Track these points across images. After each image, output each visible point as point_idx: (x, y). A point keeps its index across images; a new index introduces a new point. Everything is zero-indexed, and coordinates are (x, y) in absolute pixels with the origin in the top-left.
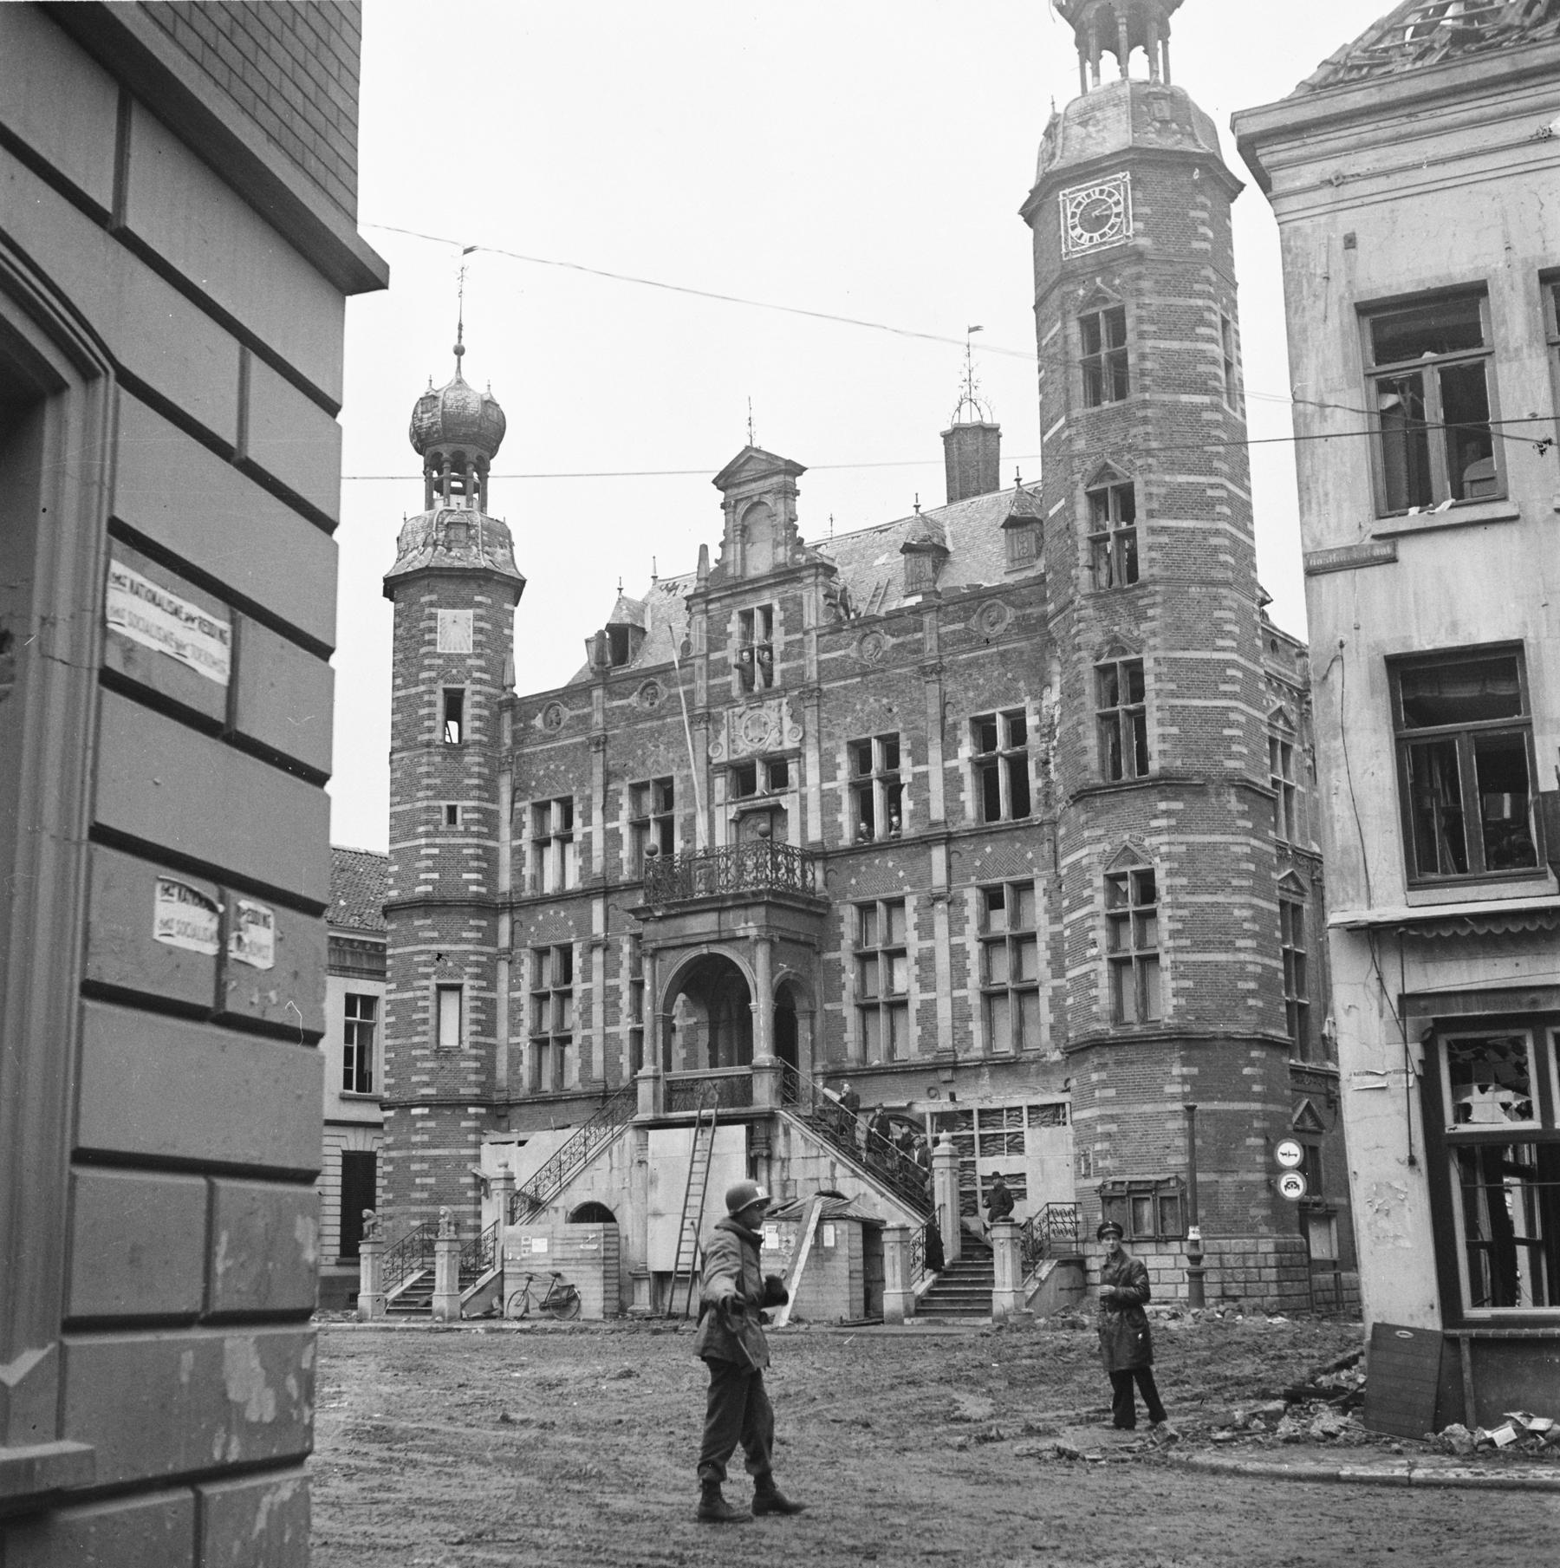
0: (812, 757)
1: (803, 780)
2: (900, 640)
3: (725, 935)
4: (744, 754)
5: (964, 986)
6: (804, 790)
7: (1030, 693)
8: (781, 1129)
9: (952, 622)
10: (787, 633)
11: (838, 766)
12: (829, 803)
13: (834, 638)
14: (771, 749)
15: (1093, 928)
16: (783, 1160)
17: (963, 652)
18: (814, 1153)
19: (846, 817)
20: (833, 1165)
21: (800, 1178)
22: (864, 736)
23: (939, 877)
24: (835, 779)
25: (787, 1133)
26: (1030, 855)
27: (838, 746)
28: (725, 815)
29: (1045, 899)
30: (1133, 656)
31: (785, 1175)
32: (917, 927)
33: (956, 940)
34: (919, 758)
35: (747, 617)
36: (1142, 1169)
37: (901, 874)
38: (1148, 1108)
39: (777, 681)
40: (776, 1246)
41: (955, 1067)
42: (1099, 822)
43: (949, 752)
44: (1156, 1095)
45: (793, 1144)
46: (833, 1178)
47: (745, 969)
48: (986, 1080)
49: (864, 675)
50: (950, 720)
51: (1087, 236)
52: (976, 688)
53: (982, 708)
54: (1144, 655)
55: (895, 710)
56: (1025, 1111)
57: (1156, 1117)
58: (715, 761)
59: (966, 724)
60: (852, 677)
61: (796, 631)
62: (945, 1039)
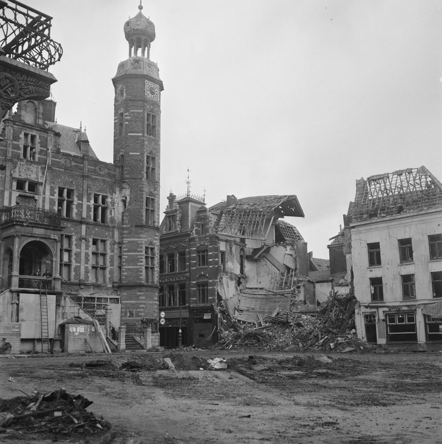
0: (48, 187)
1: (44, 193)
2: (77, 164)
3: (47, 237)
4: (23, 178)
5: (88, 264)
6: (44, 196)
7: (110, 193)
8: (63, 298)
9: (92, 166)
10: (41, 146)
11: (55, 193)
12: (52, 202)
13: (57, 155)
14: (33, 179)
15: (142, 258)
16: (63, 307)
17: (94, 175)
18: (73, 305)
19: (56, 208)
20: (79, 309)
21: (68, 312)
22: (64, 187)
23: (84, 233)
24: (54, 196)
25: (65, 299)
26: (107, 234)
27: (56, 187)
28: (15, 194)
29: (110, 246)
30: (154, 198)
31: (63, 311)
32: (76, 245)
33: (87, 251)
34: (80, 198)
35: (26, 135)
36: (149, 316)
37: (72, 229)
38: (151, 302)
39: (37, 160)
40: (83, 331)
41: (85, 285)
42: (145, 233)
43: (88, 201)
44: (152, 299)
45: (67, 302)
46: (79, 313)
47: (52, 249)
48: (92, 289)
49: (65, 169)
50: (89, 192)
51: (150, 95)
52: (96, 186)
53: (97, 191)
54: (156, 198)
55: (74, 183)
56: (109, 299)
57: (153, 305)
58: (13, 176)
59: (93, 195)
60: (62, 168)
61: (44, 147)
62: (82, 277)
